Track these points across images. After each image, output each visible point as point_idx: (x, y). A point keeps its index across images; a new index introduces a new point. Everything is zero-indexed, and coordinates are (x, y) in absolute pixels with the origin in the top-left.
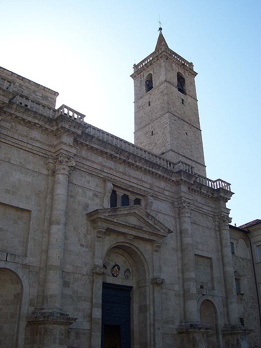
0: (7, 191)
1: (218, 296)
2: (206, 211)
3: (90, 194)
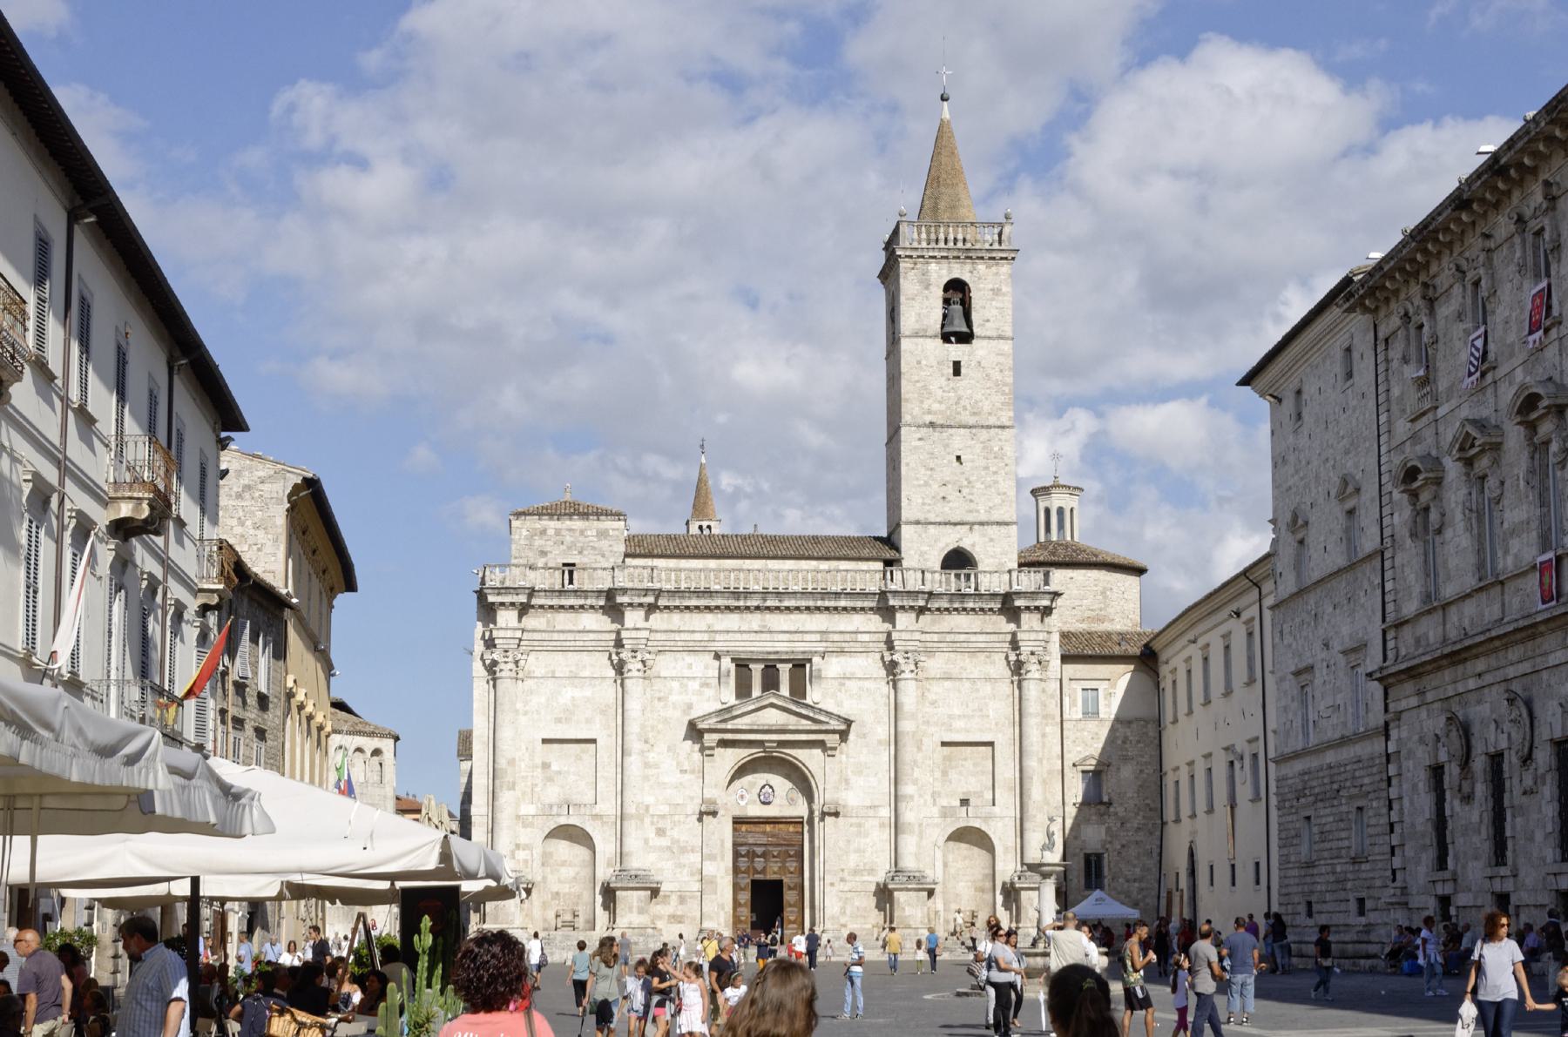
0: (559, 720)
3: (695, 685)
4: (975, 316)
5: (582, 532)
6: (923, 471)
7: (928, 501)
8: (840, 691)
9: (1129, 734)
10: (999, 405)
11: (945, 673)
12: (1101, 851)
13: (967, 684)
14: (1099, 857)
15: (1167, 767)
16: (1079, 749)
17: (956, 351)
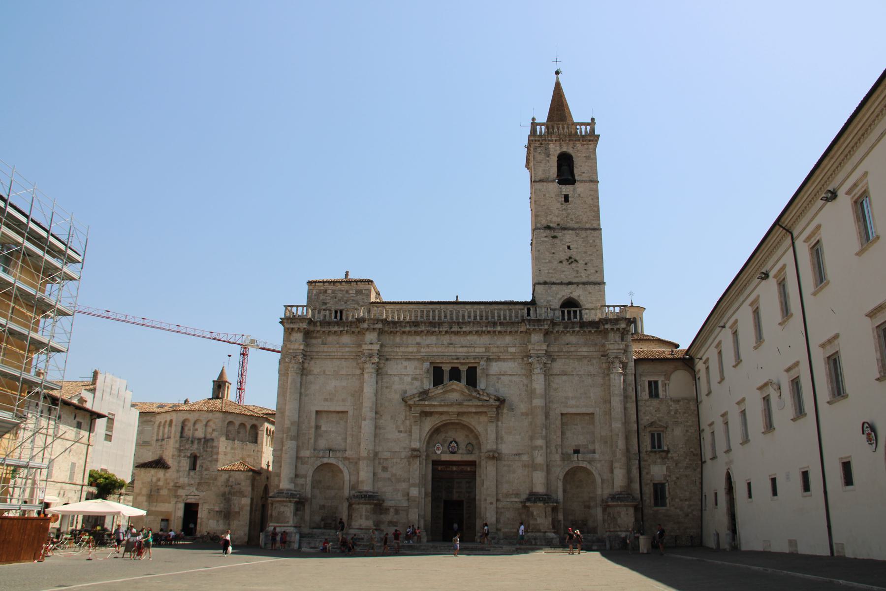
0: (326, 400)
1: (600, 461)
2: (583, 353)
3: (409, 379)
4: (576, 171)
5: (347, 292)
6: (548, 254)
7: (550, 271)
8: (498, 382)
9: (678, 408)
10: (592, 218)
11: (563, 371)
12: (664, 482)
13: (577, 378)
14: (662, 485)
15: (704, 425)
16: (647, 418)
17: (567, 189)
